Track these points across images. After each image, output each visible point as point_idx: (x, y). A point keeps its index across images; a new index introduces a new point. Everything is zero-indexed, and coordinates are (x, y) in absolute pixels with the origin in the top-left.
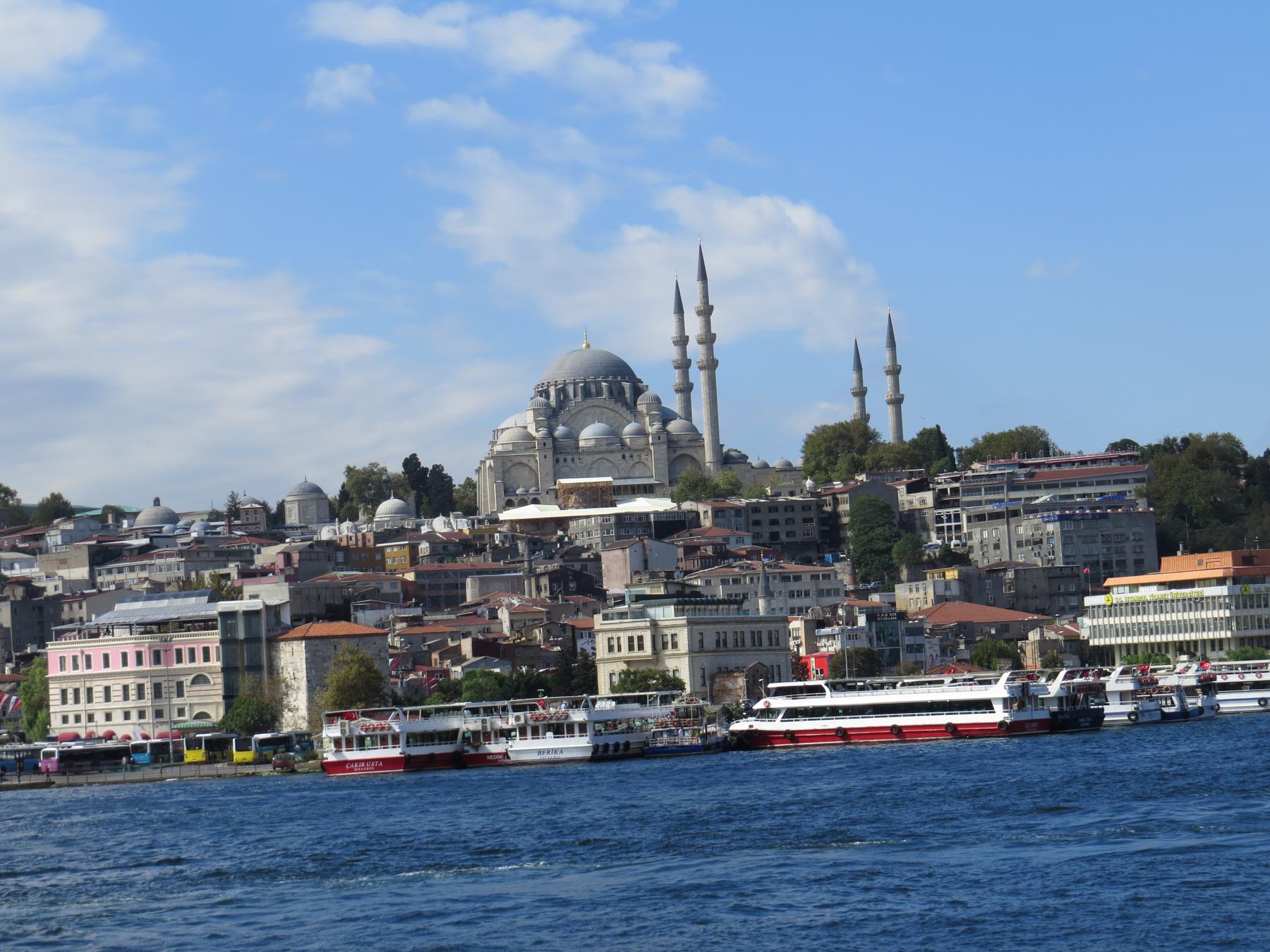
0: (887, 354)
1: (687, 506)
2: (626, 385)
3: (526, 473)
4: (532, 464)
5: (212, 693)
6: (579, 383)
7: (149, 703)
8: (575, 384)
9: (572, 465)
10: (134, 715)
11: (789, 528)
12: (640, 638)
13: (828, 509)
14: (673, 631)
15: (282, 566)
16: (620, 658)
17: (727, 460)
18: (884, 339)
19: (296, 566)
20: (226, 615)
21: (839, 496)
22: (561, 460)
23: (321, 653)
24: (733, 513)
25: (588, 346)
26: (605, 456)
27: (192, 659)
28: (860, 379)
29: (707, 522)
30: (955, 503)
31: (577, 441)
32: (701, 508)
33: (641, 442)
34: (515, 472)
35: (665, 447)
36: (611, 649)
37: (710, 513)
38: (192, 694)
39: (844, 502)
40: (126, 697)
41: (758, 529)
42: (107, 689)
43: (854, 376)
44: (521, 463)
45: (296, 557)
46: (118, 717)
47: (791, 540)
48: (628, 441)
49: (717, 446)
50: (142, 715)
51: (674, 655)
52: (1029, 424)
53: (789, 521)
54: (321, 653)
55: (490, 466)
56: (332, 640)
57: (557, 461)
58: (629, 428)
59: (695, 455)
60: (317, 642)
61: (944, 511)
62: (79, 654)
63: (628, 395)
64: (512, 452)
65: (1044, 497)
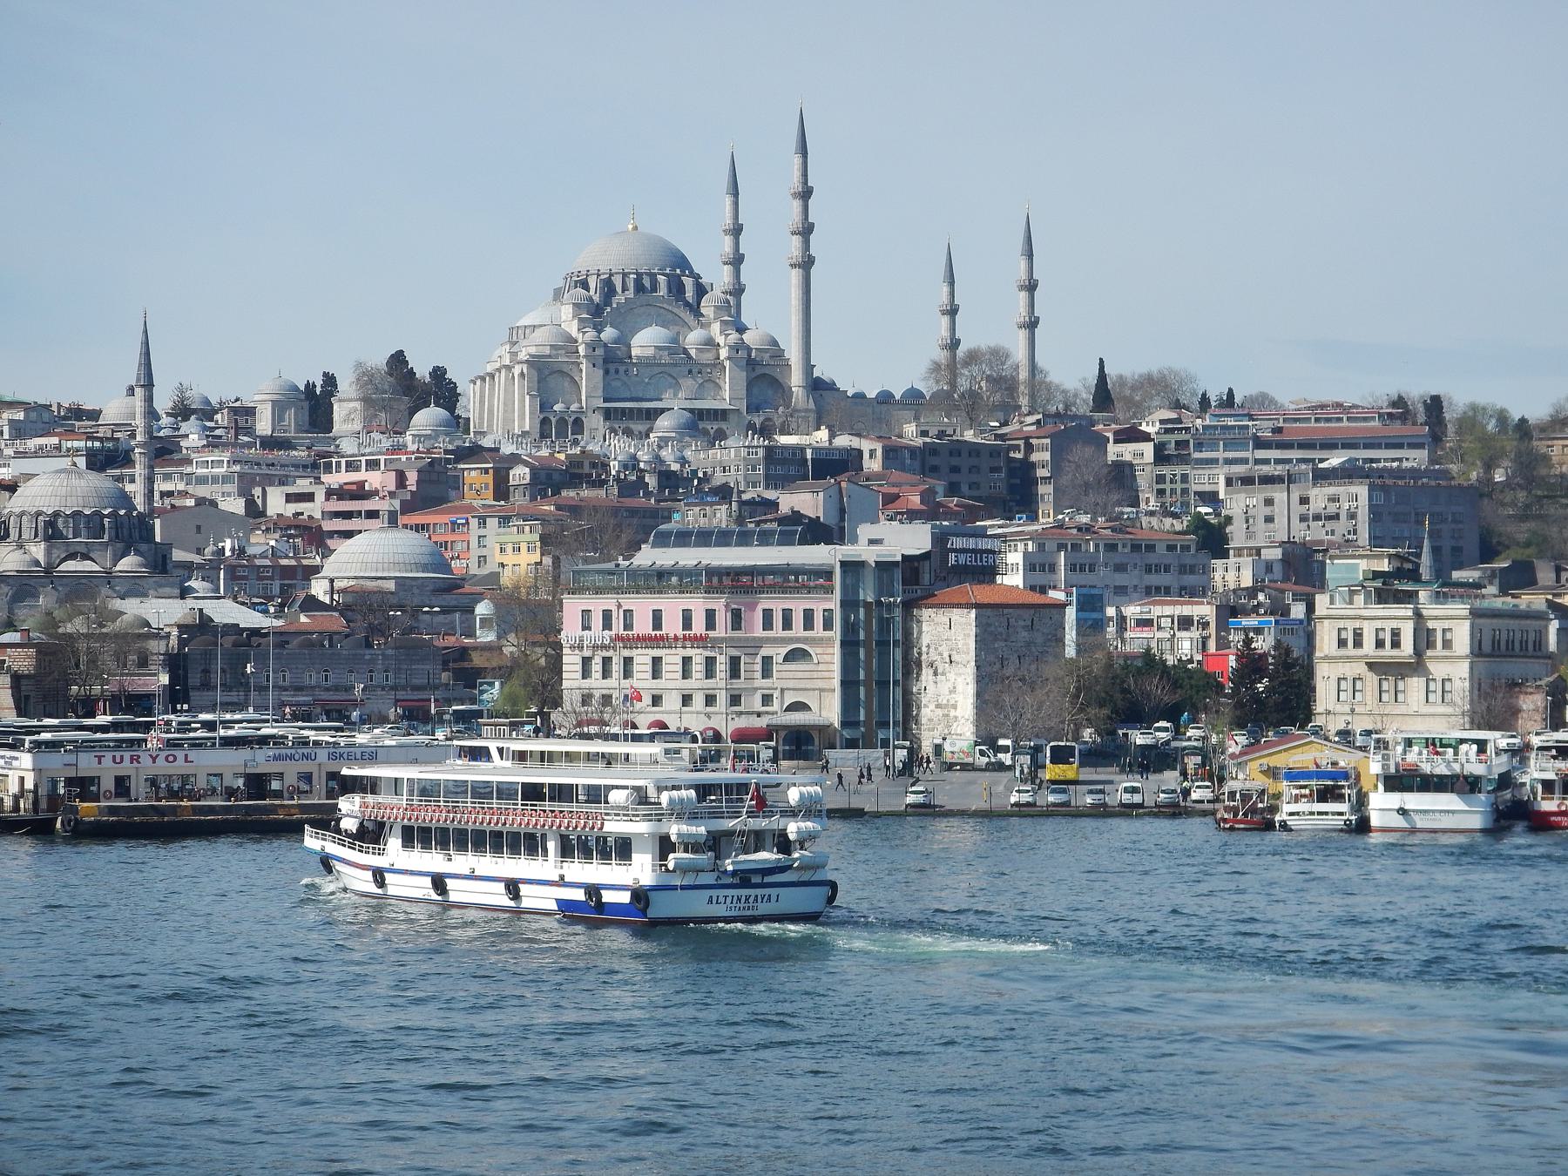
1: (843, 441)
2: (688, 282)
3: (566, 384)
5: (815, 675)
6: (630, 273)
7: (722, 684)
8: (625, 275)
9: (625, 378)
10: (698, 700)
11: (974, 478)
12: (1396, 634)
13: (1019, 456)
14: (1446, 624)
15: (392, 487)
16: (1361, 657)
17: (818, 387)
19: (414, 488)
20: (852, 568)
21: (1034, 441)
22: (612, 371)
23: (992, 629)
24: (907, 455)
25: (636, 228)
26: (667, 369)
27: (787, 624)
28: (952, 294)
29: (873, 465)
30: (1184, 460)
31: (629, 347)
32: (865, 445)
33: (707, 357)
34: (553, 381)
36: (1342, 643)
37: (879, 453)
38: (784, 675)
39: (1043, 448)
40: (686, 674)
41: (955, 477)
42: (656, 661)
43: (945, 289)
44: (561, 372)
45: (412, 478)
46: (672, 702)
47: (975, 493)
48: (693, 353)
49: (808, 368)
50: (710, 700)
51: (1446, 657)
53: (973, 469)
54: (992, 629)
55: (522, 374)
56: (1006, 611)
57: (607, 372)
58: (693, 338)
59: (779, 377)
60: (989, 612)
61: (1166, 470)
62: (614, 609)
63: (689, 294)
64: (550, 356)
65: (1335, 460)
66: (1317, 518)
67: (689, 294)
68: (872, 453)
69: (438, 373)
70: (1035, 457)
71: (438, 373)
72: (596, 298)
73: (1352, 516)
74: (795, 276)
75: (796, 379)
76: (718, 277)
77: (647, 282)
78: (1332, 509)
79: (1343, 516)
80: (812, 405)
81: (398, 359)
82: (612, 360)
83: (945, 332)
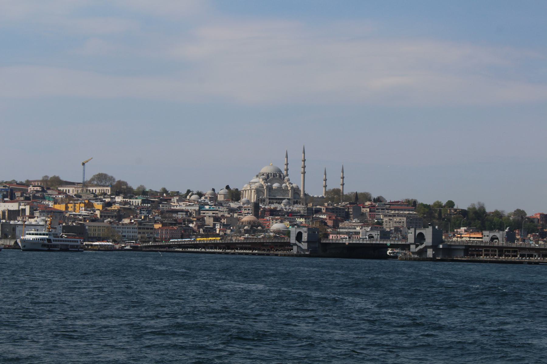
0: (342, 174)
4: (264, 191)
13: (346, 210)
17: (305, 195)
18: (341, 170)
28: (326, 177)
32: (322, 208)
35: (293, 190)
37: (325, 209)
39: (351, 209)
44: (261, 191)
49: (304, 191)
52: (367, 192)
53: (340, 212)
57: (269, 191)
58: (284, 185)
63: (282, 177)
66: (397, 222)
67: (282, 177)
68: (324, 209)
70: (350, 210)
72: (266, 177)
73: (403, 222)
74: (302, 175)
75: (302, 193)
76: (285, 173)
77: (275, 175)
78: (400, 221)
79: (402, 222)
80: (305, 198)
81: (228, 187)
82: (270, 189)
83: (324, 184)
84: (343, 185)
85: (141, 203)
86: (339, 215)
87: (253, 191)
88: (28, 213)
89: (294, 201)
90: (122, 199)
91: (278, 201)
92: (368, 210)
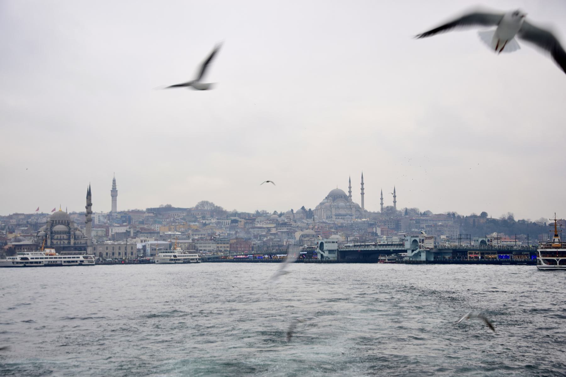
35: (354, 208)
61: (417, 225)
66: (438, 231)
68: (377, 222)
69: (310, 210)
71: (310, 210)
81: (303, 208)
84: (395, 202)
85: (231, 223)
86: (391, 226)
87: (323, 210)
88: (132, 234)
89: (356, 217)
90: (216, 220)
91: (343, 217)
92: (414, 222)
